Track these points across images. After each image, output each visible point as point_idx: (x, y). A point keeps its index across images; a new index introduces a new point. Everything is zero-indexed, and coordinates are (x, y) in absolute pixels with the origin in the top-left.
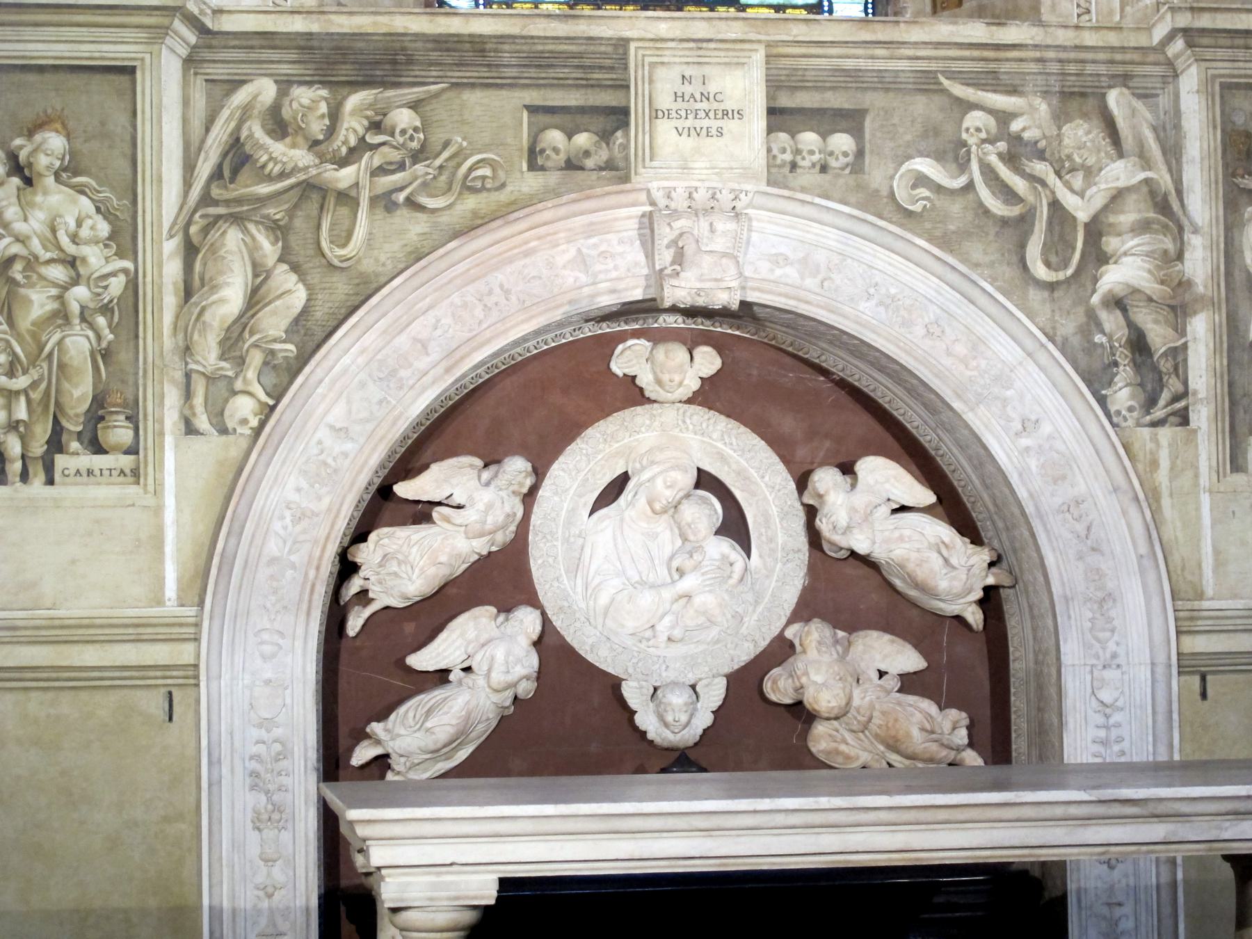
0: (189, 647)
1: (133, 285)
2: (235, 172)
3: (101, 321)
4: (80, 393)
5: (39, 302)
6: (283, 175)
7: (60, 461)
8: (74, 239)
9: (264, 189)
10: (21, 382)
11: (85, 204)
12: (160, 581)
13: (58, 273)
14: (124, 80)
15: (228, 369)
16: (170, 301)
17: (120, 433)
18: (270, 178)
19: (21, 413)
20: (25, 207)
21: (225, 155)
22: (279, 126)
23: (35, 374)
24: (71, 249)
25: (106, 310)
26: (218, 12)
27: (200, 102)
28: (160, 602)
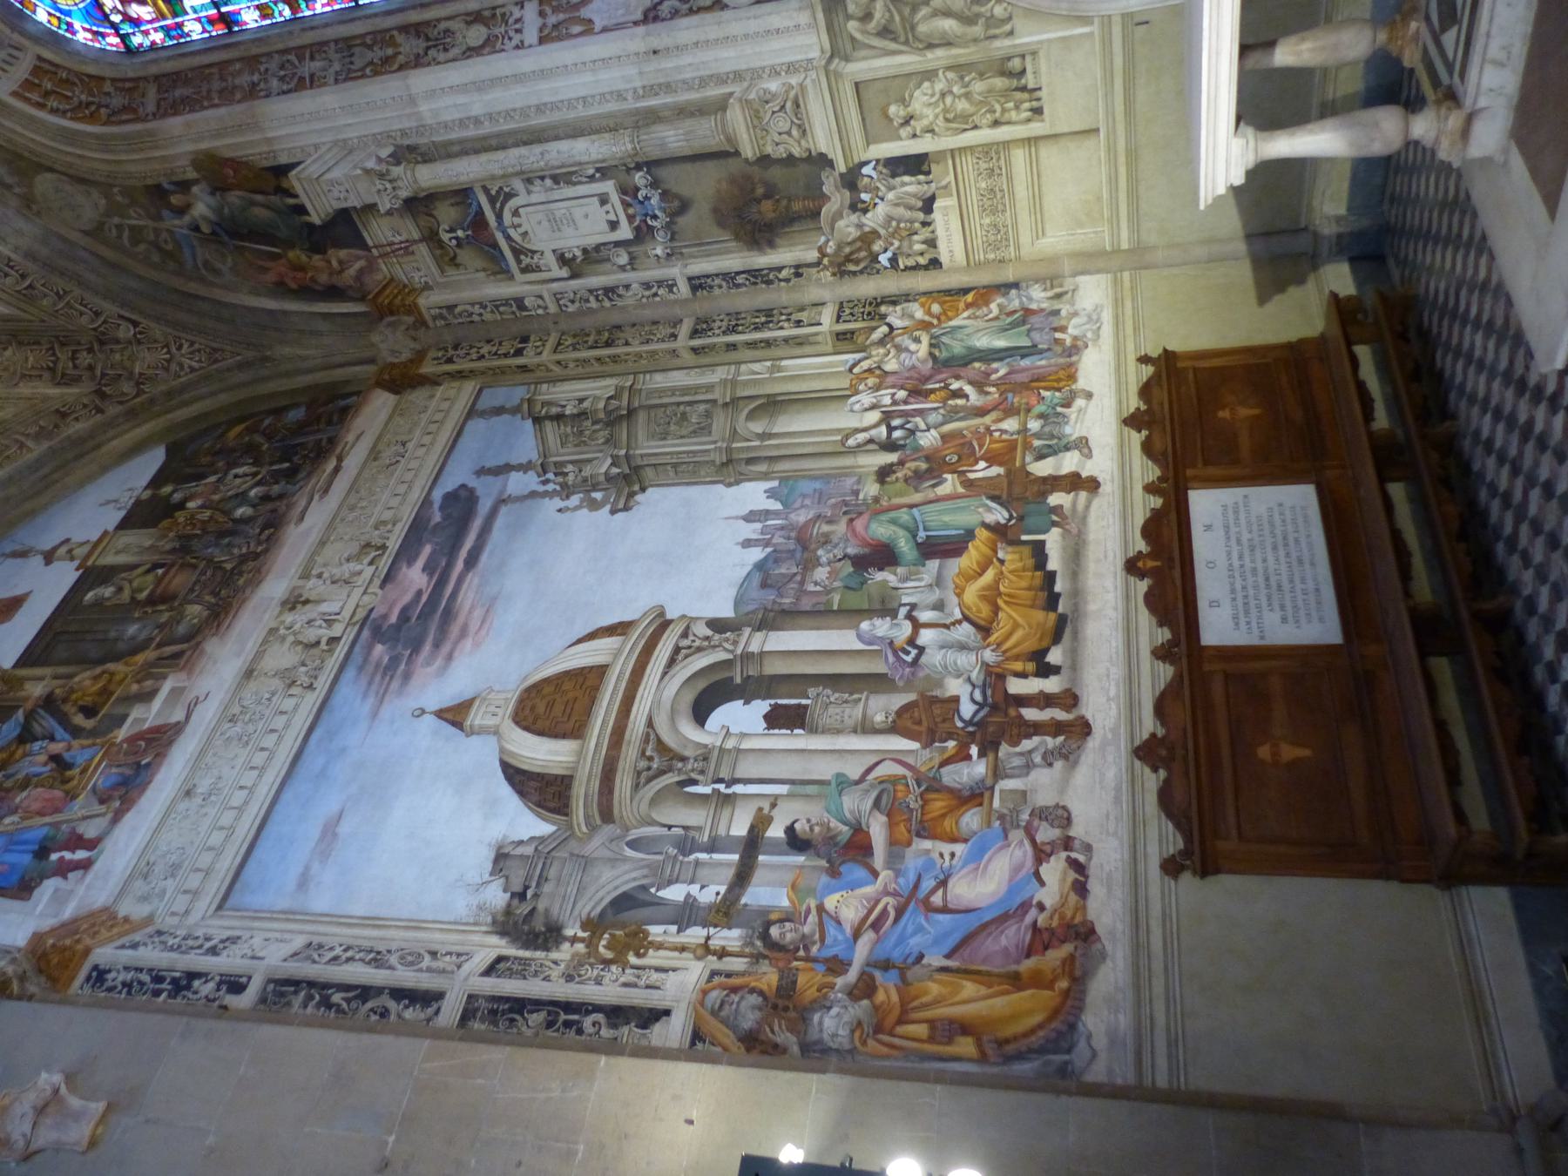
0: (1114, 19)
1: (949, 68)
2: (891, 32)
3: (967, 79)
4: (1000, 83)
5: (962, 105)
6: (889, 11)
7: (1031, 85)
8: (933, 95)
9: (897, 18)
10: (998, 107)
11: (917, 93)
12: (1081, 35)
13: (949, 100)
14: (861, 86)
15: (981, 21)
16: (955, 51)
17: (1016, 64)
18: (892, 16)
19: (1011, 105)
20: (922, 117)
21: (885, 38)
22: (867, 17)
23: (994, 103)
24: (937, 96)
25: (962, 78)
26: (823, 52)
27: (863, 53)
28: (1091, 34)
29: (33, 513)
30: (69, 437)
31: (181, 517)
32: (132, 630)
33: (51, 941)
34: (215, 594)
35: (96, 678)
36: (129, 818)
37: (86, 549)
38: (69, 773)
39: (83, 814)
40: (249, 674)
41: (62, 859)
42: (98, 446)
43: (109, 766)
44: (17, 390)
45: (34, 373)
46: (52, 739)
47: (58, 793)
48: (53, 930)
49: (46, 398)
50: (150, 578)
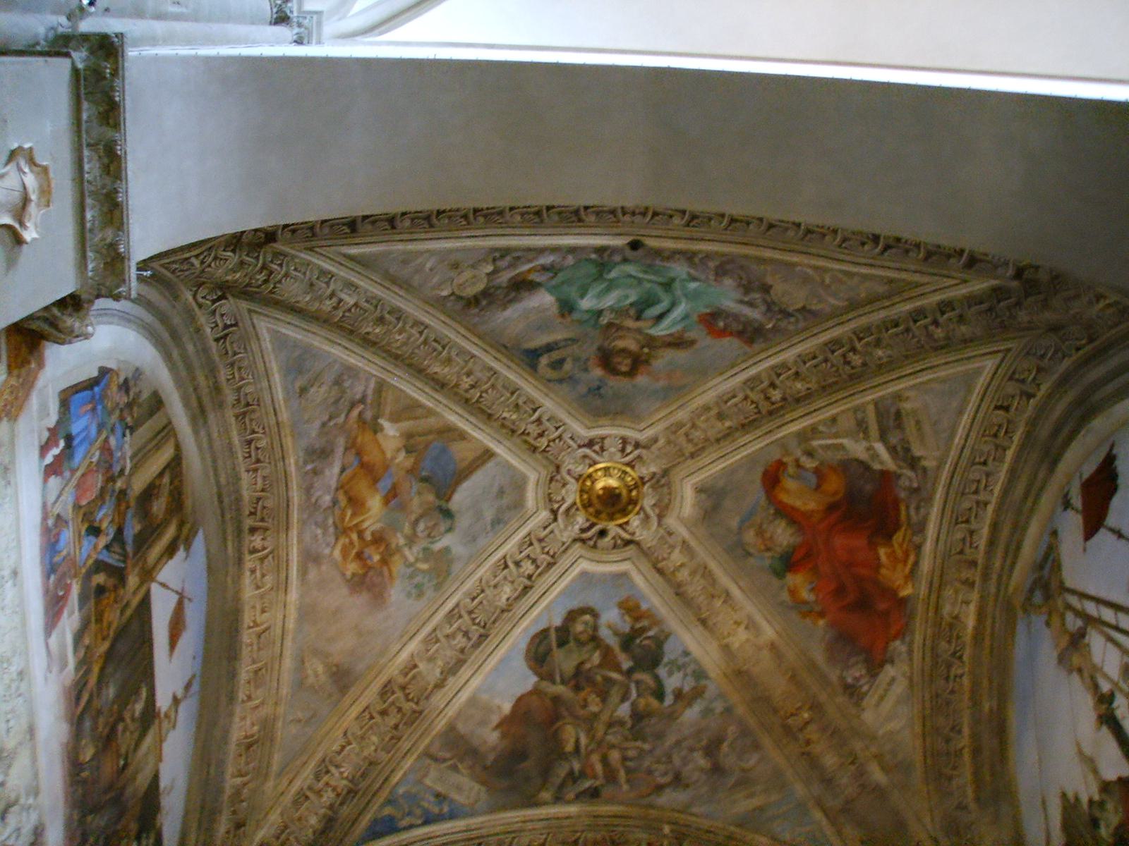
29: (199, 727)
30: (220, 812)
31: (134, 827)
32: (111, 692)
33: (33, 365)
34: (84, 782)
35: (110, 624)
36: (37, 517)
37: (164, 731)
38: (86, 526)
39: (62, 493)
40: (31, 731)
41: (57, 445)
42: (199, 827)
43: (69, 554)
44: (279, 811)
45: (283, 837)
46: (107, 547)
47: (84, 502)
48: (35, 378)
49: (258, 826)
50: (123, 751)
